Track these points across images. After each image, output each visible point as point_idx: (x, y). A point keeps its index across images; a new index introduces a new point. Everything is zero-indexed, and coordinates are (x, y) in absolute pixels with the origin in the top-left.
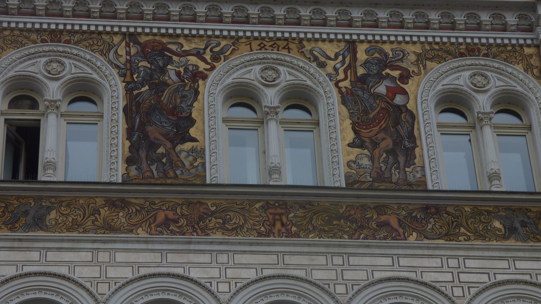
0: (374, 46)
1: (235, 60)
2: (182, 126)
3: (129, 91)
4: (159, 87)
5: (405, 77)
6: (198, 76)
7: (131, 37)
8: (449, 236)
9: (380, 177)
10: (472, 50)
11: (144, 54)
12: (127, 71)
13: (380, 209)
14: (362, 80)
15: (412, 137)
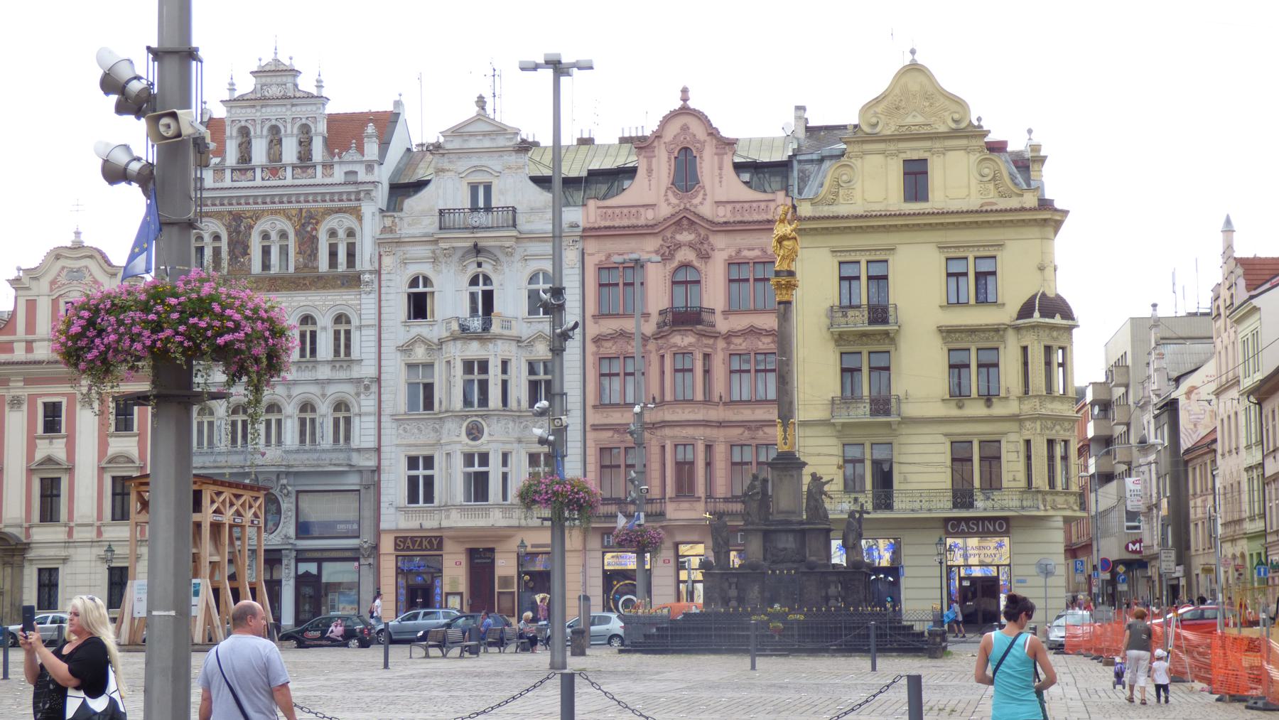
0: (309, 211)
1: (263, 220)
2: (246, 252)
3: (229, 235)
4: (238, 233)
5: (317, 223)
6: (251, 227)
7: (230, 212)
8: (324, 288)
9: (306, 266)
10: (340, 210)
11: (234, 219)
12: (228, 227)
13: (304, 278)
14: (303, 225)
15: (317, 249)
